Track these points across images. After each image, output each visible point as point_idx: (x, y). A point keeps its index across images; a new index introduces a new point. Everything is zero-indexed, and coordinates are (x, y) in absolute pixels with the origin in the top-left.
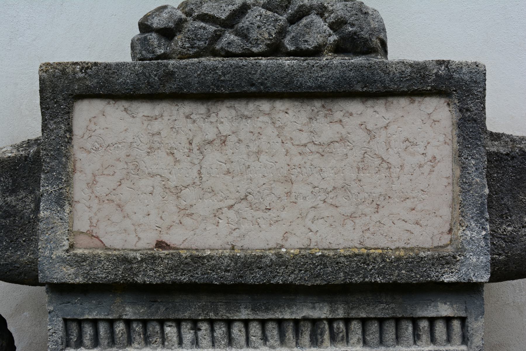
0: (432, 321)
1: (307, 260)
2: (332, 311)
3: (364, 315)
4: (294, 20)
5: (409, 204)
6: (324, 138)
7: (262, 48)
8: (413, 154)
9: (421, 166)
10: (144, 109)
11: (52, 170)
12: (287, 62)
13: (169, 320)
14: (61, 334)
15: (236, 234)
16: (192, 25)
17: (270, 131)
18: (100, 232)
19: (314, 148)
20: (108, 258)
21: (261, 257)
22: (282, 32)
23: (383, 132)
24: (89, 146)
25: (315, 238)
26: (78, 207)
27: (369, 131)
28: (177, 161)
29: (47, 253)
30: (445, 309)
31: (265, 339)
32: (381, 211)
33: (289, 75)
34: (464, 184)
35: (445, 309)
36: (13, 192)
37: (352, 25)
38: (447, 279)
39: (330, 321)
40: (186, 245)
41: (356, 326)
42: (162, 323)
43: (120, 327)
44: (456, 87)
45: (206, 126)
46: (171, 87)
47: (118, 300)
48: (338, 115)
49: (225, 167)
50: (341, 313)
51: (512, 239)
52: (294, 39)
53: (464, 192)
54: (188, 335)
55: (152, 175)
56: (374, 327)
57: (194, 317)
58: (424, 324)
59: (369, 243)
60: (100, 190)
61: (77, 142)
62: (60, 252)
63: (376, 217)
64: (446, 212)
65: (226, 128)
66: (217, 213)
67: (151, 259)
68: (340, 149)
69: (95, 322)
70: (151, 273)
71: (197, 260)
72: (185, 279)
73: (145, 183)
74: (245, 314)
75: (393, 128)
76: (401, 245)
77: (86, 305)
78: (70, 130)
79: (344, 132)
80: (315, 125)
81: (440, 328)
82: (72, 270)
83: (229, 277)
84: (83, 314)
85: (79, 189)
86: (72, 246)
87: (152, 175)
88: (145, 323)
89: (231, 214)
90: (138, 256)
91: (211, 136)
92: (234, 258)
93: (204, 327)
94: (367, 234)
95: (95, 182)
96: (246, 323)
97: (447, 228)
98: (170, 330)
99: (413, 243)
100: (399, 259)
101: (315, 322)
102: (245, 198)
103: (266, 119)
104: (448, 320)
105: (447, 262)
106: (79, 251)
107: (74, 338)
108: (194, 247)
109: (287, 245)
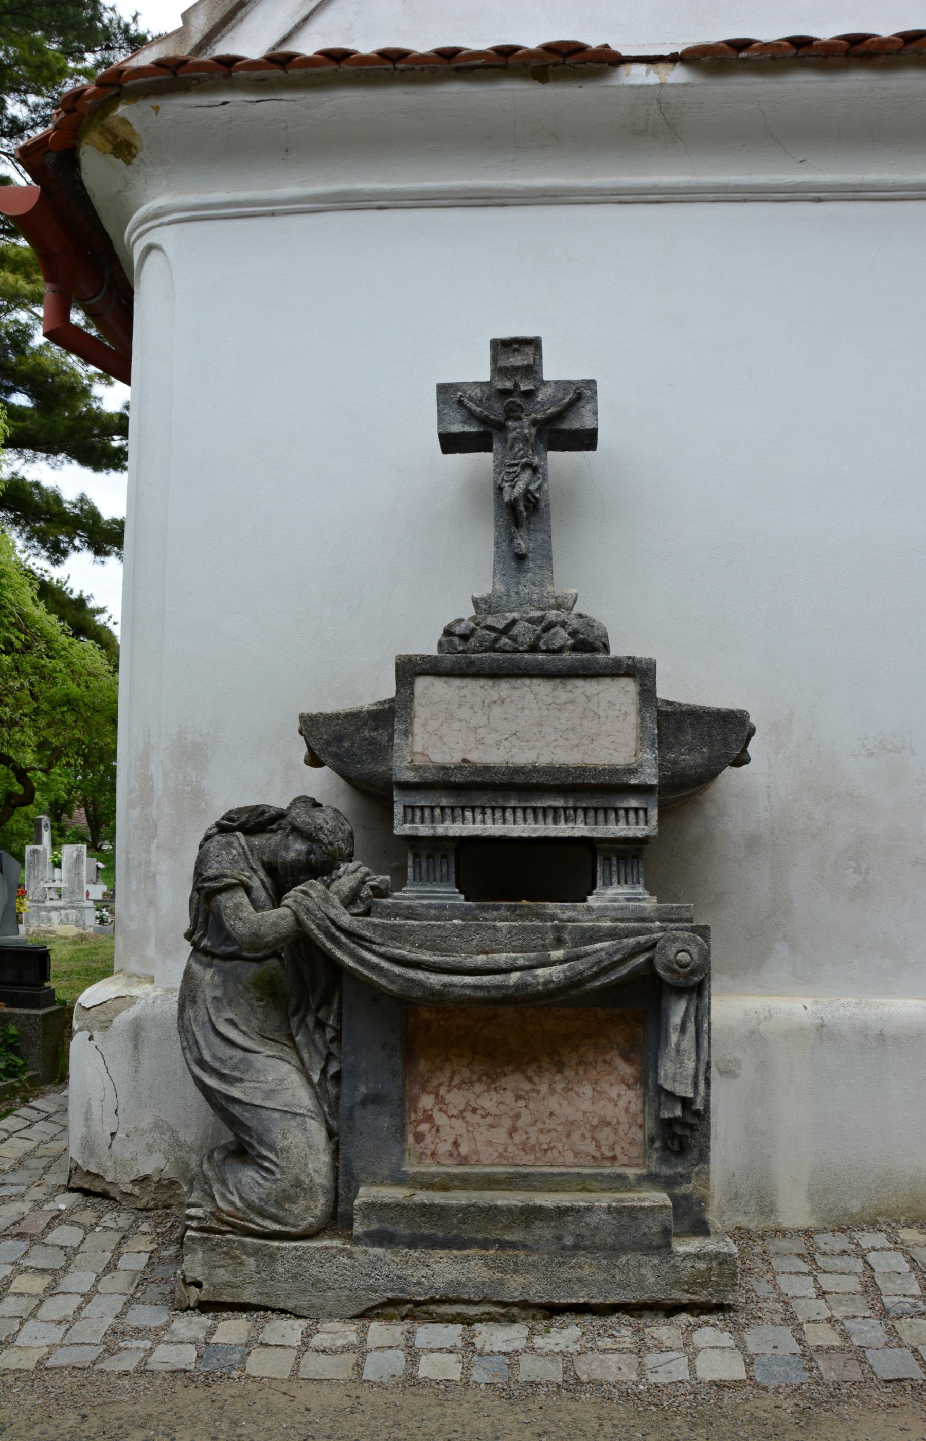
0: (627, 810)
1: (550, 770)
2: (566, 802)
3: (585, 805)
4: (546, 629)
5: (610, 739)
6: (561, 700)
7: (525, 647)
8: (613, 710)
9: (618, 717)
10: (456, 682)
11: (402, 716)
12: (540, 656)
13: (468, 807)
14: (402, 814)
15: (509, 755)
16: (481, 632)
17: (530, 696)
18: (429, 753)
19: (555, 706)
20: (434, 767)
22: (538, 638)
23: (596, 697)
24: (423, 703)
25: (555, 758)
26: (417, 738)
27: (587, 697)
28: (475, 712)
29: (398, 764)
30: (634, 803)
31: (525, 820)
32: (595, 743)
33: (541, 664)
34: (643, 727)
35: (634, 803)
36: (375, 730)
37: (583, 634)
38: (633, 781)
39: (565, 809)
40: (480, 761)
41: (580, 813)
42: (463, 809)
43: (437, 812)
44: (641, 672)
45: (492, 692)
46: (473, 670)
48: (569, 687)
49: (503, 716)
50: (571, 804)
51: (675, 762)
52: (546, 643)
53: (643, 732)
54: (479, 817)
55: (460, 720)
56: (591, 813)
57: (483, 805)
58: (622, 813)
59: (587, 761)
60: (430, 728)
61: (416, 700)
62: (406, 764)
63: (591, 746)
64: (633, 744)
65: (504, 694)
66: (498, 743)
67: (459, 768)
68: (570, 707)
69: (422, 808)
71: (487, 768)
72: (479, 779)
73: (456, 725)
74: (513, 803)
75: (601, 695)
76: (606, 762)
77: (418, 797)
78: (412, 693)
79: (572, 697)
80: (555, 692)
81: (632, 815)
82: (412, 774)
83: (505, 779)
85: (417, 727)
86: (412, 761)
87: (460, 720)
88: (453, 809)
89: (507, 743)
91: (495, 698)
92: (508, 768)
93: (489, 812)
94: (586, 756)
95: (426, 723)
96: (514, 809)
97: (633, 753)
98: (468, 814)
99: (613, 762)
100: (604, 770)
101: (555, 810)
102: (515, 734)
103: (527, 689)
104: (636, 810)
105: (632, 771)
107: (409, 818)
109: (539, 761)
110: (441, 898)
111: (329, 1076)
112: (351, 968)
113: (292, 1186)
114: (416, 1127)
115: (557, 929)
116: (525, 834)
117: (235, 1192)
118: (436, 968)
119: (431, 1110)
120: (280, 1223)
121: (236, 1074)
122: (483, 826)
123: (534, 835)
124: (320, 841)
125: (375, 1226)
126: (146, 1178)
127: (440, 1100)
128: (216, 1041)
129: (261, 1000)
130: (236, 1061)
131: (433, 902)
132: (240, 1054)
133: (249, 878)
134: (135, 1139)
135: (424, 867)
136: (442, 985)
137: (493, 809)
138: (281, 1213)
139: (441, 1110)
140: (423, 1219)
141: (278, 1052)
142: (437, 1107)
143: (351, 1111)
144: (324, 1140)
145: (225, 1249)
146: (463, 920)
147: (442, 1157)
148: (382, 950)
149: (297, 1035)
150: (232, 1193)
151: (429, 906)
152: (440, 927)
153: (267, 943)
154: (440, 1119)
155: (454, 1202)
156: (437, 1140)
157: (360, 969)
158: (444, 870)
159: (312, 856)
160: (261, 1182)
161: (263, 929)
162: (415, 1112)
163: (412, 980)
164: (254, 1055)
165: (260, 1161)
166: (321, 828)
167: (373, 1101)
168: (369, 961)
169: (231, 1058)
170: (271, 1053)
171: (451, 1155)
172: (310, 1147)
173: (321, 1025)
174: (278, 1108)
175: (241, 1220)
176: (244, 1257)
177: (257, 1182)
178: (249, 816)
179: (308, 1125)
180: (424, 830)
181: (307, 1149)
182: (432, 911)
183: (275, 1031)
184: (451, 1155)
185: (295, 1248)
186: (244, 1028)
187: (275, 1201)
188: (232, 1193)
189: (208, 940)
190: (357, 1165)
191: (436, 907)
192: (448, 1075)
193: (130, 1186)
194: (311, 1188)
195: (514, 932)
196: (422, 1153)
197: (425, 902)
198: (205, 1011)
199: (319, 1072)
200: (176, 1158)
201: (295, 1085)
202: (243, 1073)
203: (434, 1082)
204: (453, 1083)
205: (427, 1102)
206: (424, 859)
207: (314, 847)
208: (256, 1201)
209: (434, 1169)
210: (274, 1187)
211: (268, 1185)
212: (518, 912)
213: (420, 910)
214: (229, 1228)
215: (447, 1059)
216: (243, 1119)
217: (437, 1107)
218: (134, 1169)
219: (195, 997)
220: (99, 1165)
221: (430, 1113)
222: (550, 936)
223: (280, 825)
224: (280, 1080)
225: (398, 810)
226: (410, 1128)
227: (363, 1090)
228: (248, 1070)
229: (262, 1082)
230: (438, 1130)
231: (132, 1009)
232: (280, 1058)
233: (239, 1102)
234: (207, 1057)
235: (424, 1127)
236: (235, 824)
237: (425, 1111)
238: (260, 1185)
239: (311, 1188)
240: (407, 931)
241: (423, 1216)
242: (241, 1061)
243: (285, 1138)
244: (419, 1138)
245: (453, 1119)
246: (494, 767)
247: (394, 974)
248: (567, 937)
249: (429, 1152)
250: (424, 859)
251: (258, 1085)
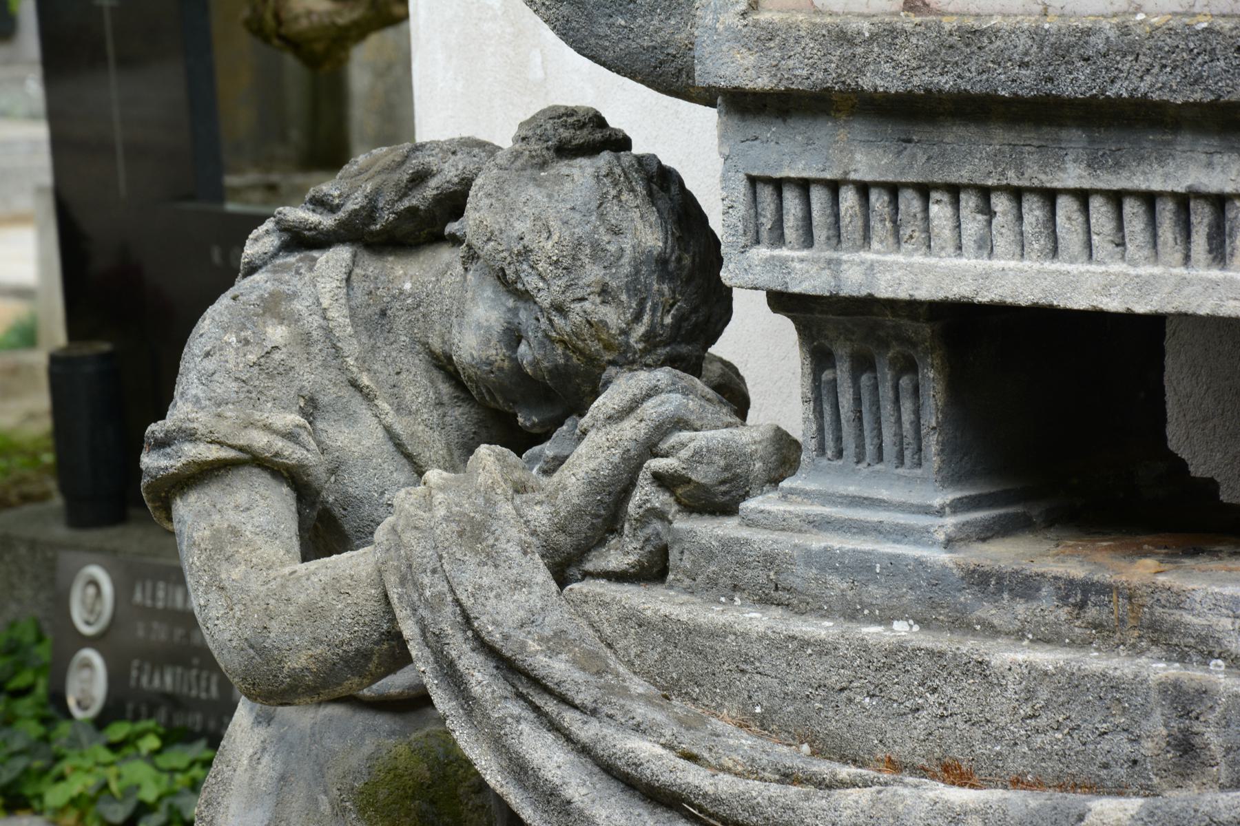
21: (1088, 32)
29: (708, 20)
42: (924, 191)
43: (849, 199)
54: (973, 224)
57: (979, 180)
69: (804, 185)
70: (887, 68)
72: (946, 82)
74: (1073, 176)
82: (751, 60)
83: (1027, 83)
88: (893, 190)
90: (866, 27)
92: (1037, 35)
93: (1001, 203)
96: (1083, 197)
98: (940, 211)
106: (763, 17)
108: (973, 9)
115: (1184, 702)
116: (1113, 304)
122: (983, 263)
123: (1140, 309)
137: (1017, 194)
146: (924, 623)
151: (827, 562)
153: (295, 676)
157: (516, 798)
158: (907, 417)
159: (523, 348)
161: (274, 626)
166: (527, 251)
178: (377, 191)
182: (833, 579)
195: (1043, 694)
197: (817, 542)
206: (842, 373)
212: (1092, 613)
213: (800, 575)
222: (1157, 727)
236: (328, 221)
240: (731, 656)
246: (995, 33)
248: (1212, 738)
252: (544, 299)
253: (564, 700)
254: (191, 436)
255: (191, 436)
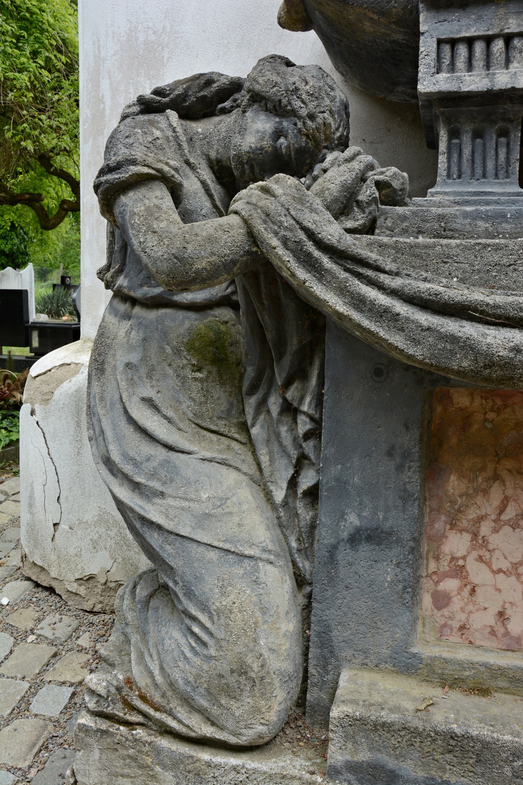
14: (434, 55)
47: (502, 11)
77: (464, 21)
84: (460, 31)
107: (446, 61)
110: (497, 203)
111: (300, 491)
112: (340, 316)
113: (232, 671)
114: (437, 583)
117: (155, 657)
118: (499, 317)
119: (464, 558)
120: (213, 724)
121: (155, 484)
124: (294, 113)
125: (364, 756)
126: (91, 578)
127: (479, 542)
128: (129, 431)
129: (199, 370)
130: (155, 464)
131: (483, 208)
132: (162, 453)
133: (176, 170)
134: (79, 532)
135: (467, 152)
136: (512, 349)
138: (215, 711)
139: (480, 559)
140: (448, 757)
141: (220, 452)
142: (475, 554)
143: (333, 549)
144: (287, 596)
145: (131, 751)
147: (478, 635)
148: (396, 283)
149: (253, 425)
150: (151, 656)
151: (476, 216)
152: (497, 248)
153: (198, 272)
154: (478, 573)
155: (508, 738)
156: (470, 607)
157: (356, 316)
158: (502, 156)
159: (282, 140)
160: (189, 655)
161: (190, 247)
162: (437, 558)
163: (453, 339)
164: (180, 455)
165: (187, 621)
166: (297, 89)
167: (369, 539)
168: (372, 303)
169: (148, 460)
170: (208, 455)
171: (493, 633)
172: (264, 611)
173: (290, 410)
174: (215, 544)
175: (157, 709)
176: (158, 769)
177: (183, 653)
179: (261, 575)
180: (474, 82)
181: (258, 614)
182: (480, 223)
183: (219, 418)
184: (493, 633)
185: (234, 768)
186: (170, 413)
187: (207, 690)
188: (151, 656)
189: (125, 277)
190: (338, 635)
191: (487, 217)
192: (496, 503)
193: (75, 585)
194: (262, 678)
196: (445, 625)
198: (114, 384)
199: (285, 485)
200: (124, 559)
201: (245, 507)
202: (164, 483)
203: (472, 514)
204: (504, 517)
205: (456, 544)
206: (466, 139)
207: (285, 124)
208: (181, 682)
209: (464, 654)
210: (205, 667)
211: (197, 661)
213: (460, 223)
214: (139, 719)
215: (496, 477)
216: (164, 555)
217: (475, 554)
218: (79, 567)
219: (103, 363)
220: (43, 557)
221: (461, 563)
223: (235, 101)
224: (221, 499)
225: (427, 47)
226: (427, 584)
227: (353, 520)
228: (172, 480)
229: (192, 500)
230: (473, 591)
231: (74, 379)
232: (223, 463)
233: (159, 527)
234: (116, 457)
235: (450, 585)
237: (453, 559)
238: (186, 658)
239: (262, 678)
240: (438, 256)
241: (450, 752)
242: (161, 465)
243: (224, 594)
244: (441, 600)
245: (501, 576)
247: (420, 326)
249: (456, 625)
250: (466, 139)
251: (185, 504)
252: (304, 112)
253: (378, 269)
254: (134, 162)
255: (134, 162)
